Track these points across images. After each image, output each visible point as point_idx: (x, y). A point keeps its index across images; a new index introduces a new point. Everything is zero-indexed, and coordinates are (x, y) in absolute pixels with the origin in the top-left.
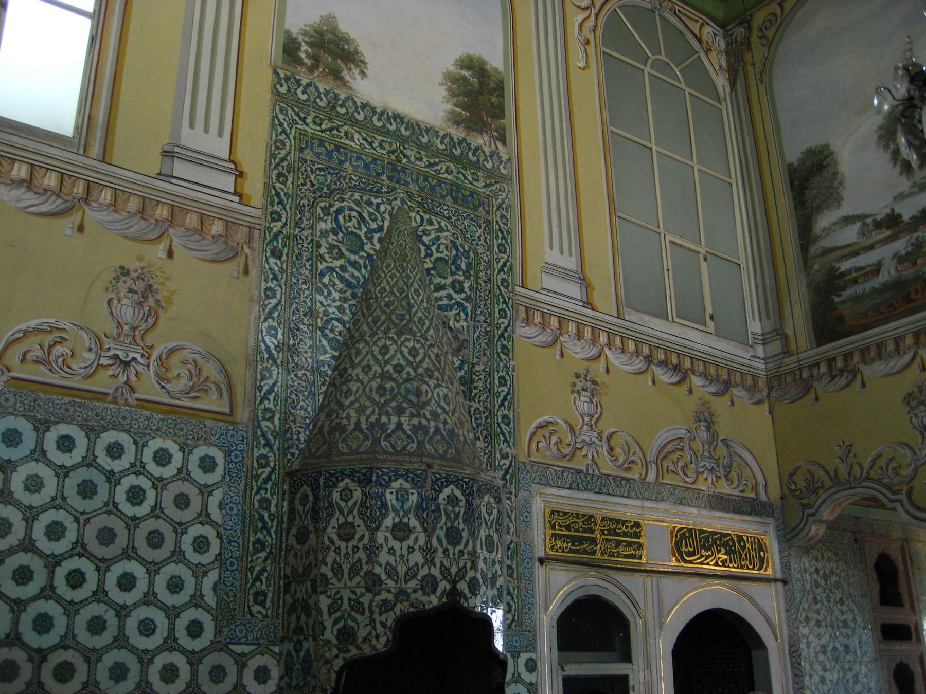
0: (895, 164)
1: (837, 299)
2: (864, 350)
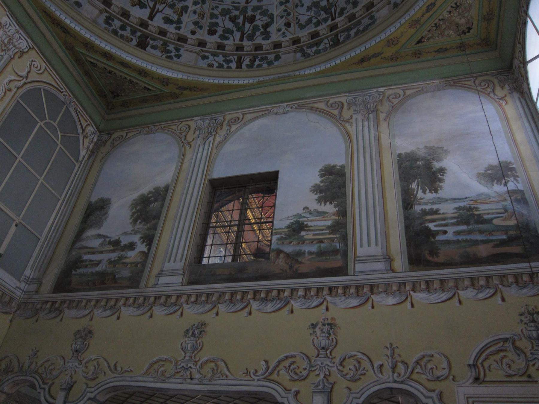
0: (131, 218)
1: (74, 272)
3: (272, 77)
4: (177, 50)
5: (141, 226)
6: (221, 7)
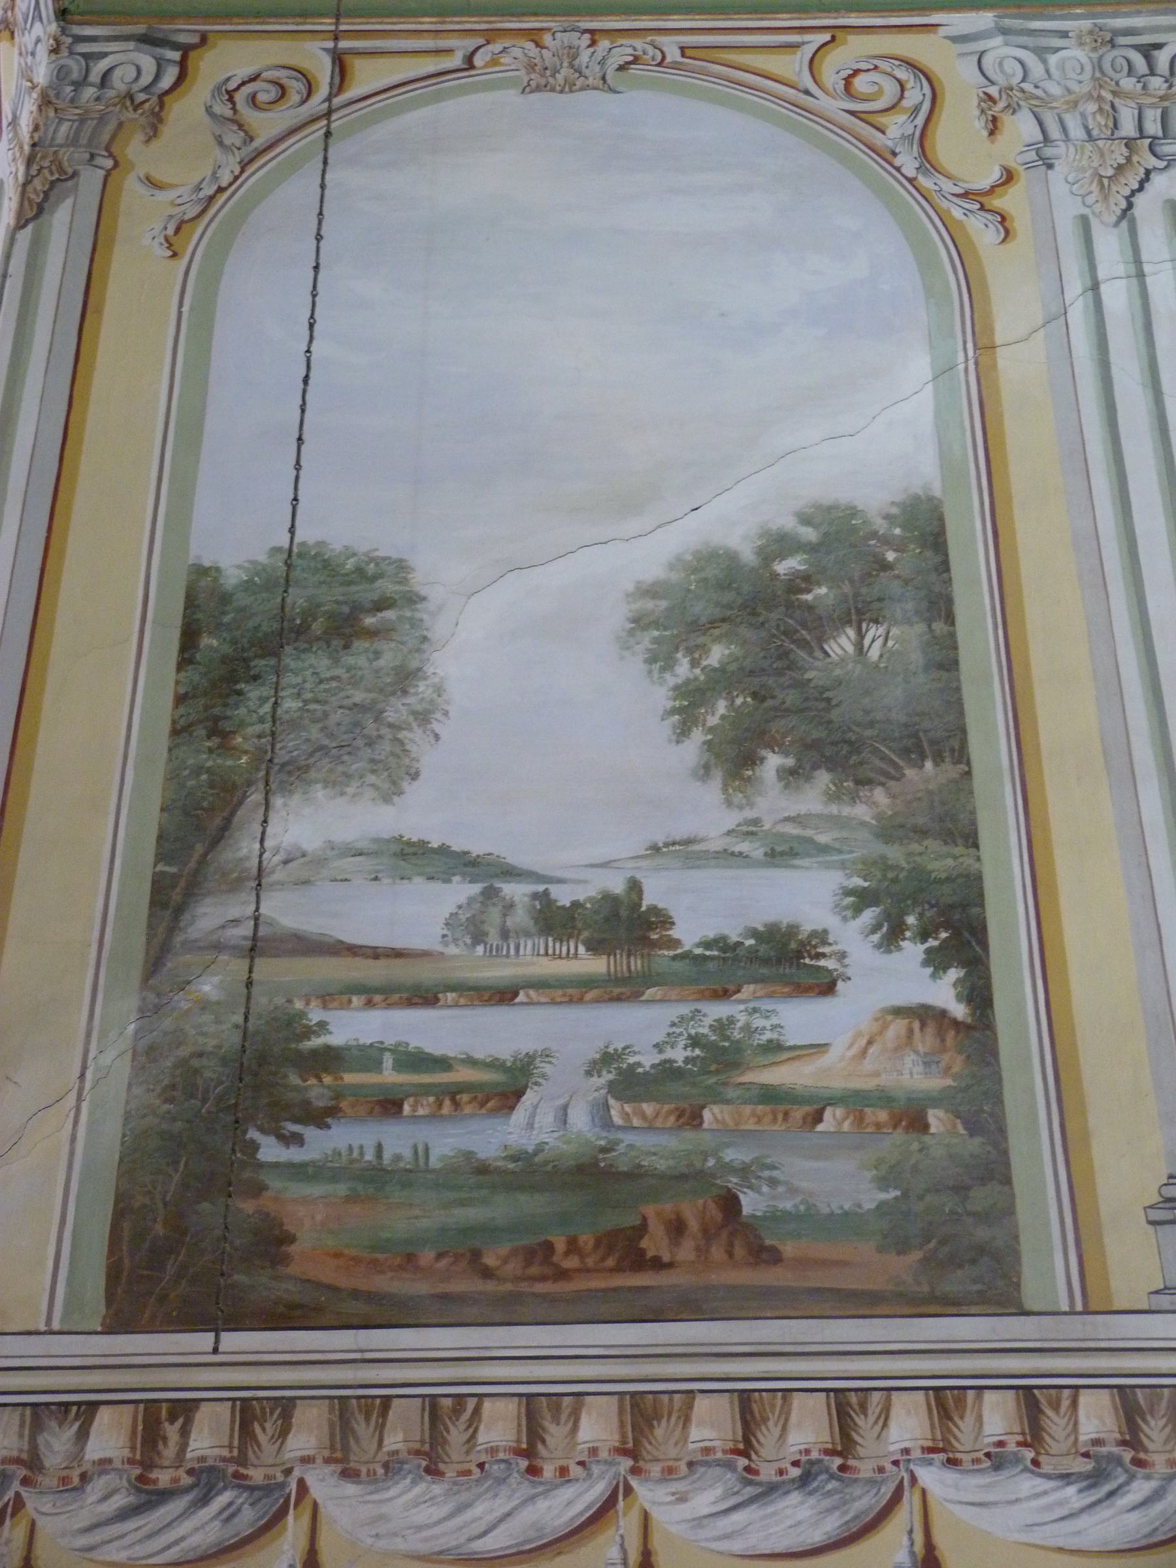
0: (682, 733)
1: (270, 1150)
2: (355, 1414)
5: (812, 799)
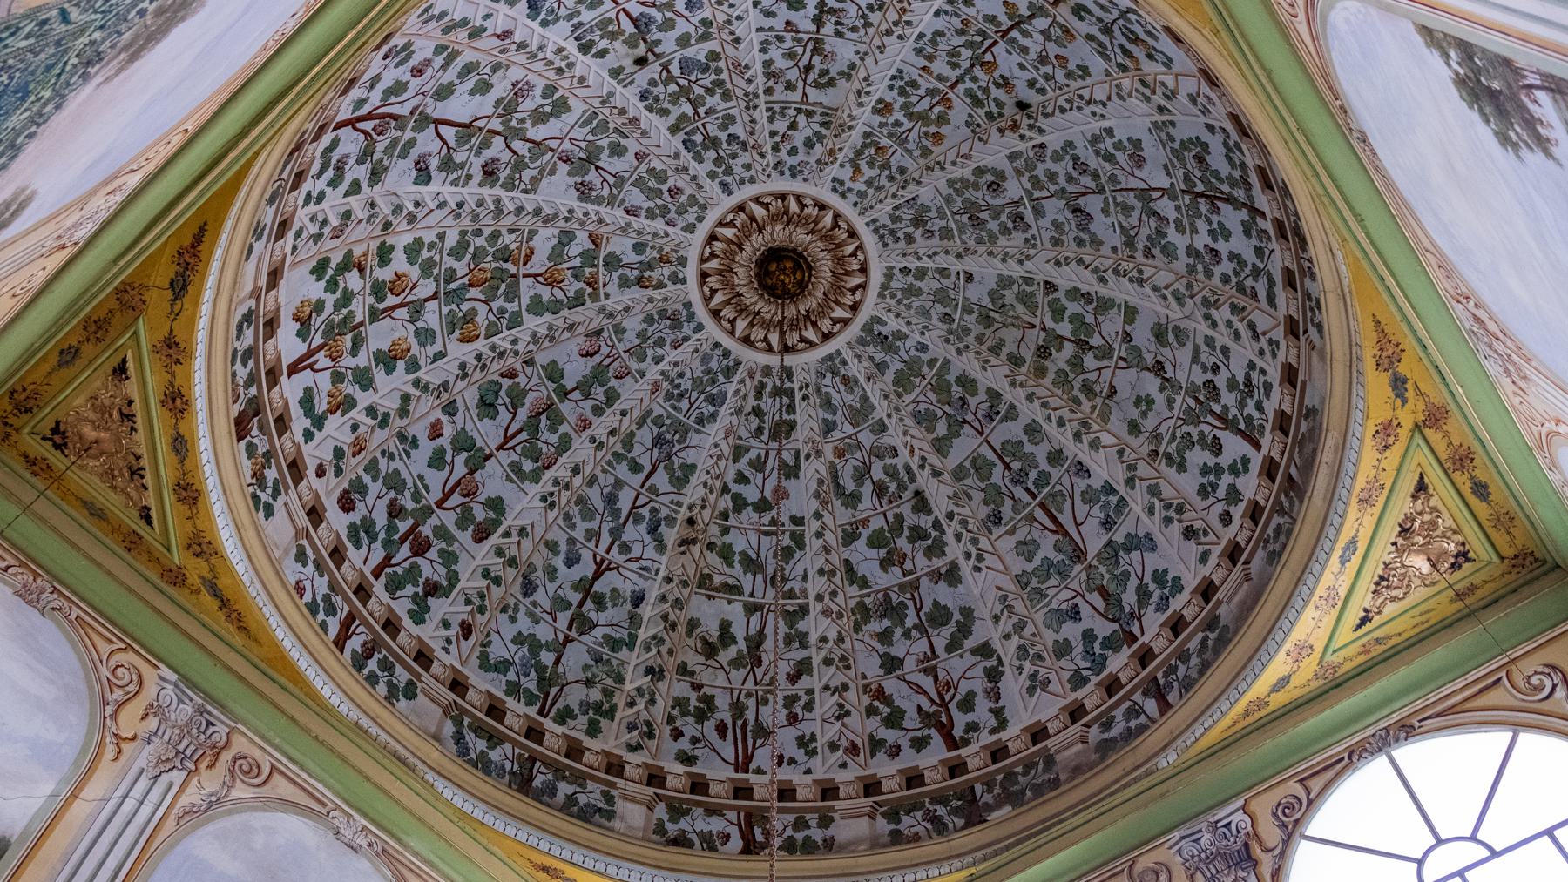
3: (383, 737)
4: (276, 493)
6: (398, 464)
